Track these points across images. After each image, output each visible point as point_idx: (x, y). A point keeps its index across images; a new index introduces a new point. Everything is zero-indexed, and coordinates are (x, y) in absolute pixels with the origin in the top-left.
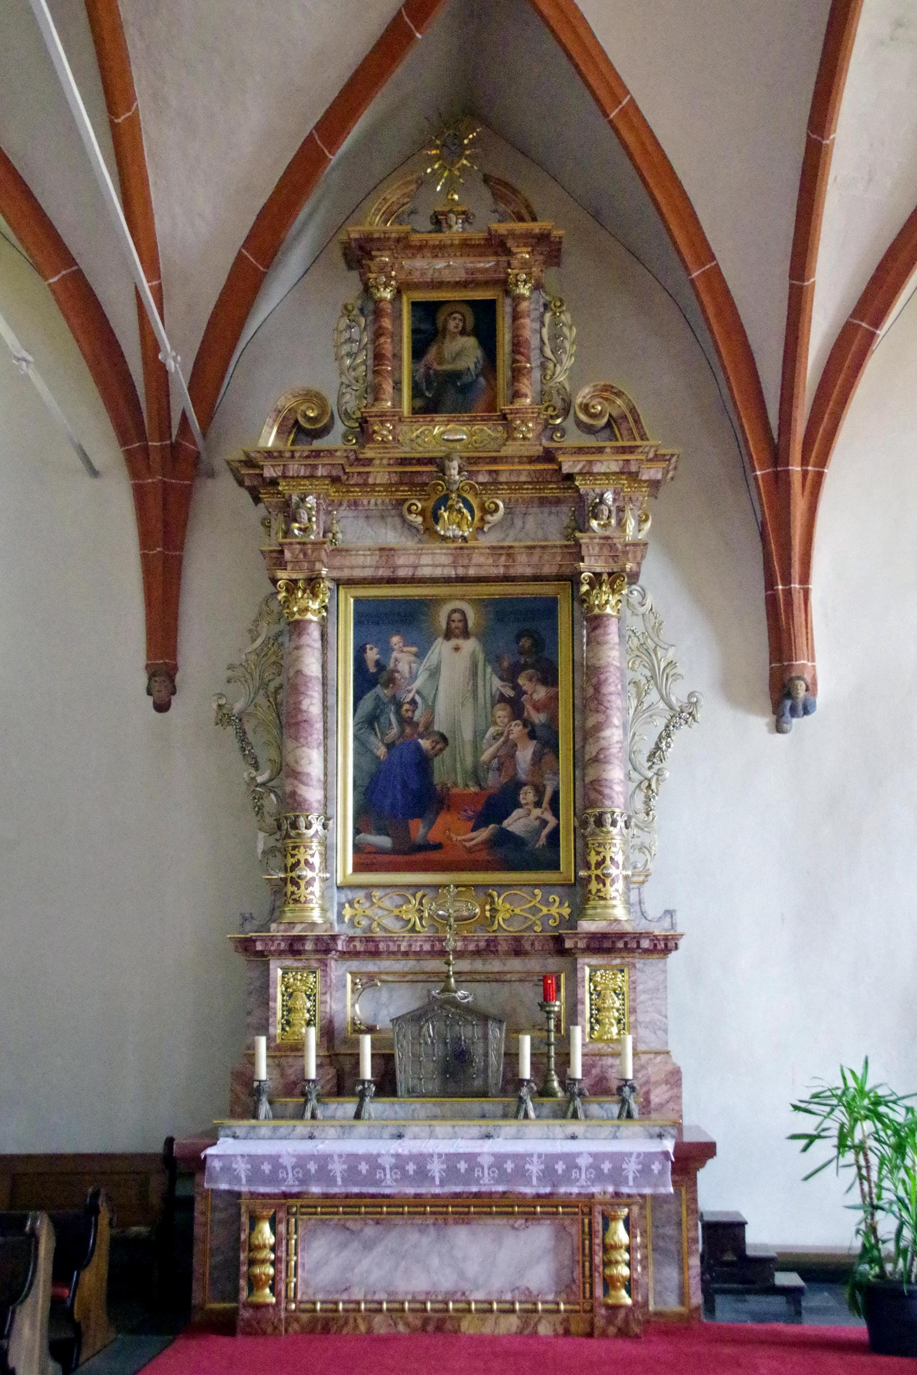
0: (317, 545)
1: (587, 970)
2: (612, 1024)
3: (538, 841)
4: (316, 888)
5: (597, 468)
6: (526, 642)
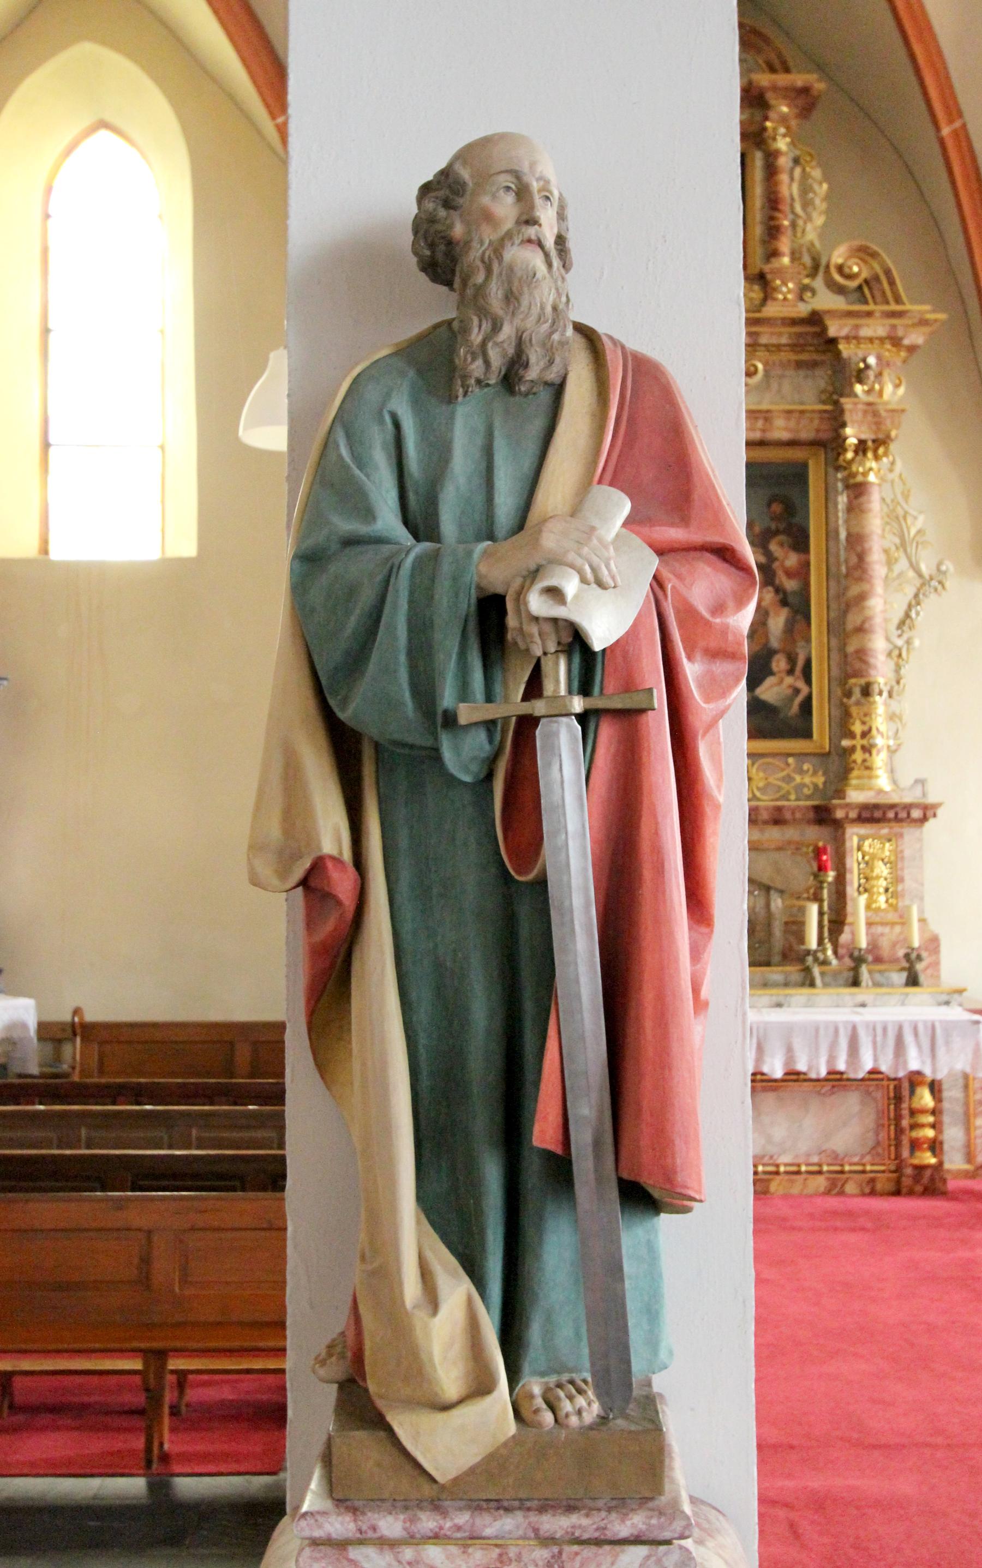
1: (855, 839)
2: (879, 893)
3: (790, 708)
5: (865, 332)
6: (777, 508)
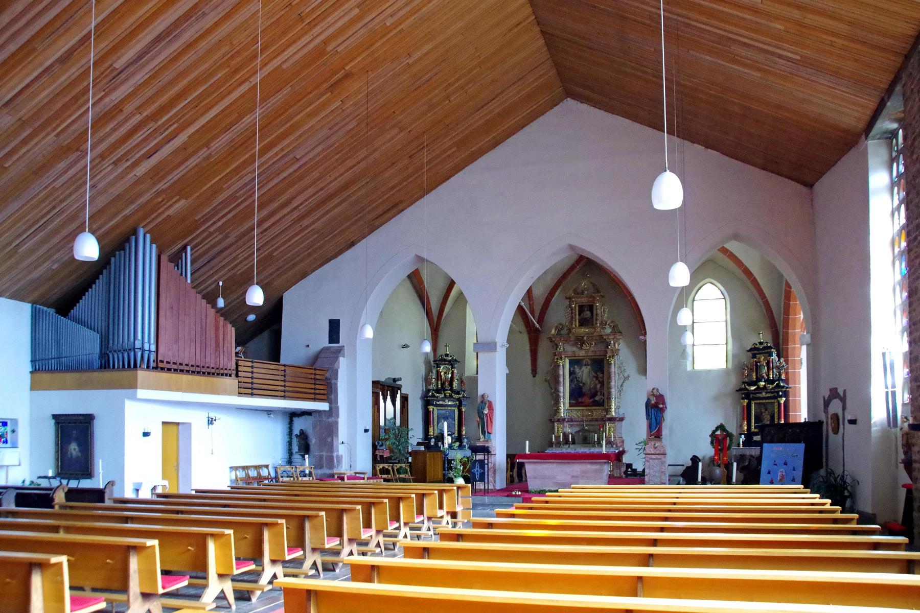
0: (562, 352)
4: (562, 410)
